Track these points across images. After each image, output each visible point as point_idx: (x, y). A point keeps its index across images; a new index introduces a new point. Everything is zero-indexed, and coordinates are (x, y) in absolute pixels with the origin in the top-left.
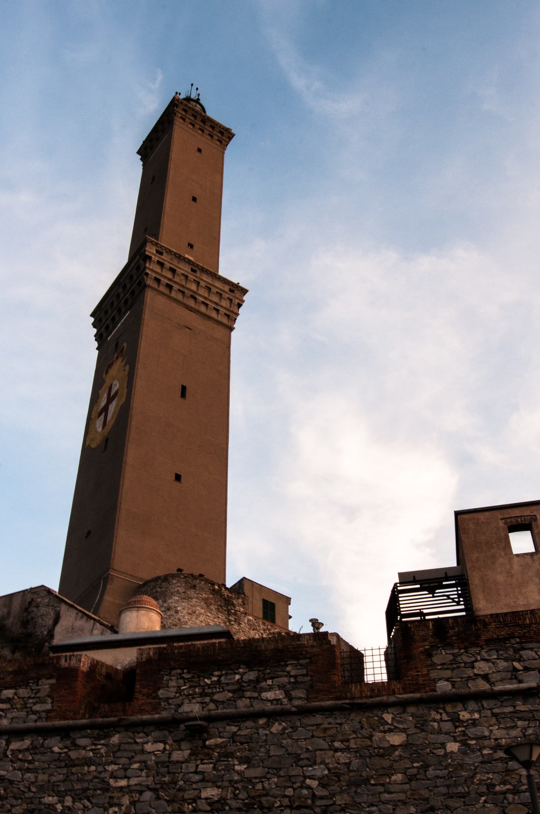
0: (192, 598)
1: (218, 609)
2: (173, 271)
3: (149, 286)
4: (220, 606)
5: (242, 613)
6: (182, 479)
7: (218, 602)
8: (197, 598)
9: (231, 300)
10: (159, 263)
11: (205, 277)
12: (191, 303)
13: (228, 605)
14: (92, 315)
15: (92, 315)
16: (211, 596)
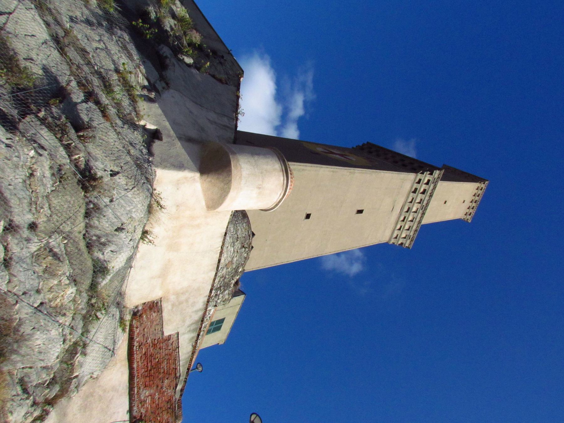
0: (233, 246)
1: (222, 277)
2: (423, 193)
3: (417, 175)
4: (225, 278)
5: (216, 302)
6: (307, 220)
7: (229, 275)
8: (234, 251)
9: (405, 238)
10: (429, 181)
11: (420, 215)
12: (406, 209)
13: (224, 286)
14: (367, 142)
15: (367, 142)
16: (234, 267)
